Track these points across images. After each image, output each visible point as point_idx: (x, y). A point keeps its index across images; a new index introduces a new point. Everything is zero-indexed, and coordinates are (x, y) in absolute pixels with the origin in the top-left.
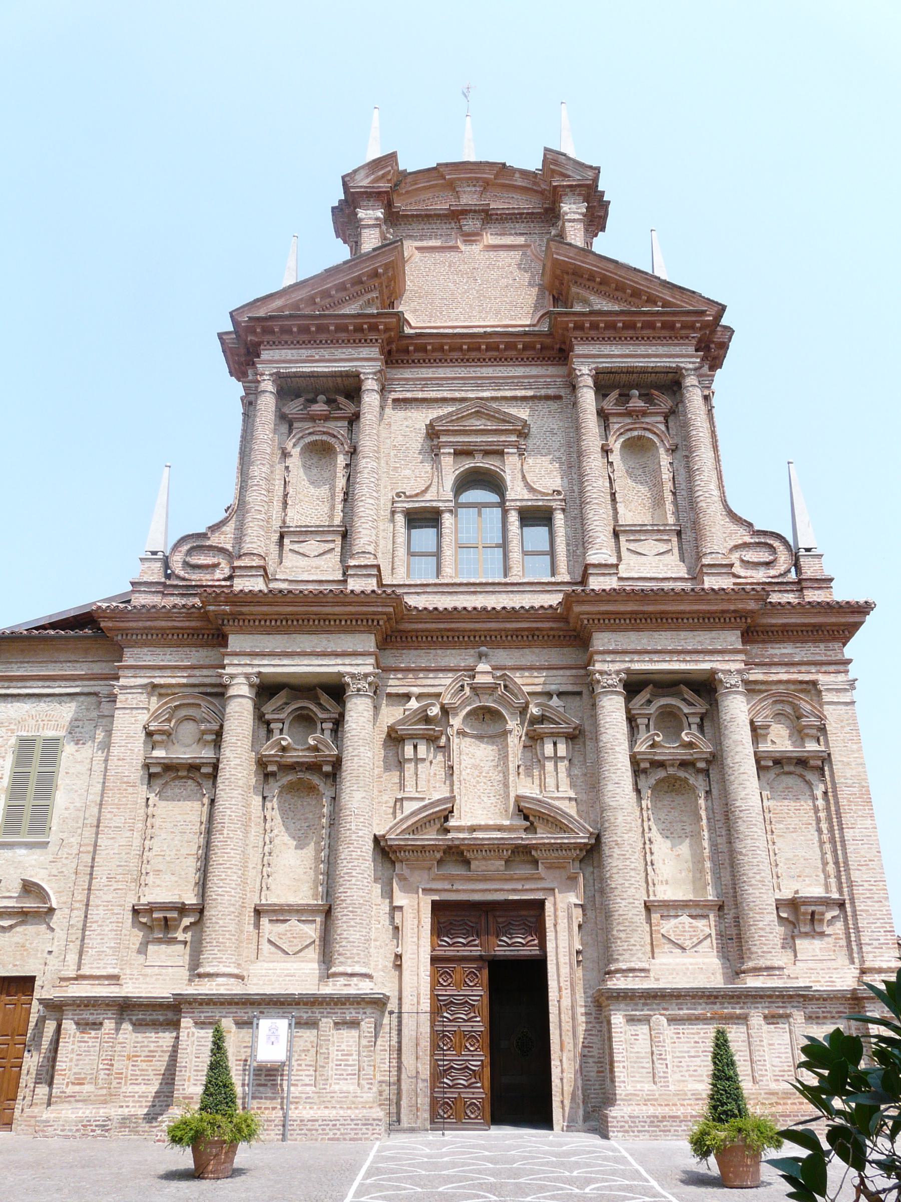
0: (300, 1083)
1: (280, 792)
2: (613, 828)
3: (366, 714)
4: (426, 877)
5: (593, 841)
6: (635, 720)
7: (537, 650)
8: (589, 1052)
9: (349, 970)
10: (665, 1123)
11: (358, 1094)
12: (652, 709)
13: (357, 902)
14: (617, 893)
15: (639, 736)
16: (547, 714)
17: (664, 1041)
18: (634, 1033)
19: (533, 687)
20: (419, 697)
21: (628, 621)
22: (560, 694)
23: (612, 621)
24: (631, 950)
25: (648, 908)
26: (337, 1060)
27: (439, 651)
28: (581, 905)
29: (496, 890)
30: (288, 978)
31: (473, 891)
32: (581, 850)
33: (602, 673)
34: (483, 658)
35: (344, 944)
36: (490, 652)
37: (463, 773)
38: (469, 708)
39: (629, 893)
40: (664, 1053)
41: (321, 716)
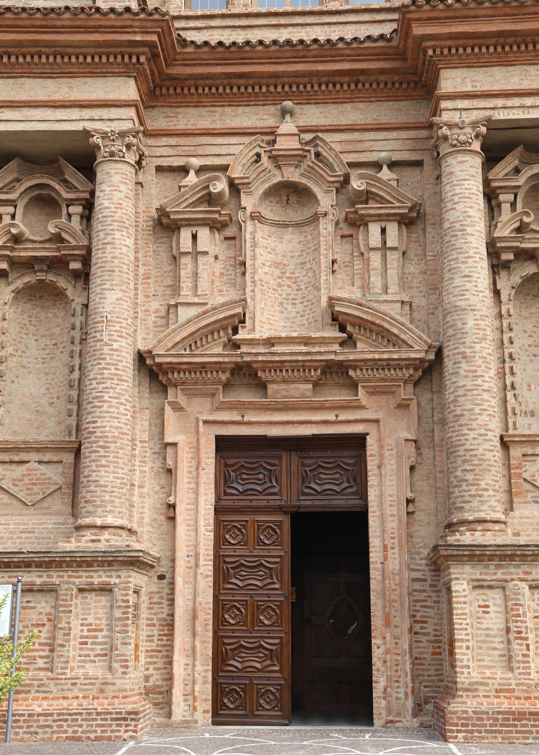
0: (31, 667)
1: (15, 298)
2: (459, 335)
3: (123, 187)
4: (209, 406)
5: (432, 357)
6: (497, 197)
7: (361, 105)
8: (422, 628)
9: (99, 522)
10: (524, 722)
11: (109, 681)
12: (521, 180)
13: (110, 435)
14: (463, 421)
15: (500, 219)
16: (373, 190)
17: (524, 615)
18: (482, 604)
19: (355, 155)
20: (201, 170)
21: (492, 49)
22: (393, 165)
23: (469, 50)
24: (481, 496)
25: (505, 444)
26: (82, 637)
27: (228, 110)
28: (415, 441)
29: (301, 423)
30: (24, 535)
31: (270, 423)
32: (416, 369)
33: (450, 126)
34: (288, 117)
35: (92, 488)
36: (297, 109)
37: (260, 270)
38: (267, 185)
39: (480, 422)
40: (524, 630)
41: (66, 195)
